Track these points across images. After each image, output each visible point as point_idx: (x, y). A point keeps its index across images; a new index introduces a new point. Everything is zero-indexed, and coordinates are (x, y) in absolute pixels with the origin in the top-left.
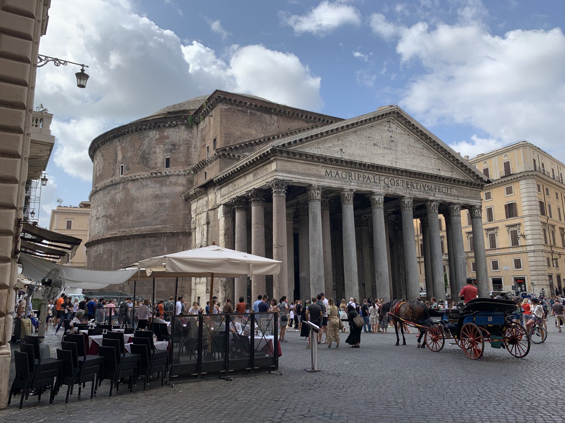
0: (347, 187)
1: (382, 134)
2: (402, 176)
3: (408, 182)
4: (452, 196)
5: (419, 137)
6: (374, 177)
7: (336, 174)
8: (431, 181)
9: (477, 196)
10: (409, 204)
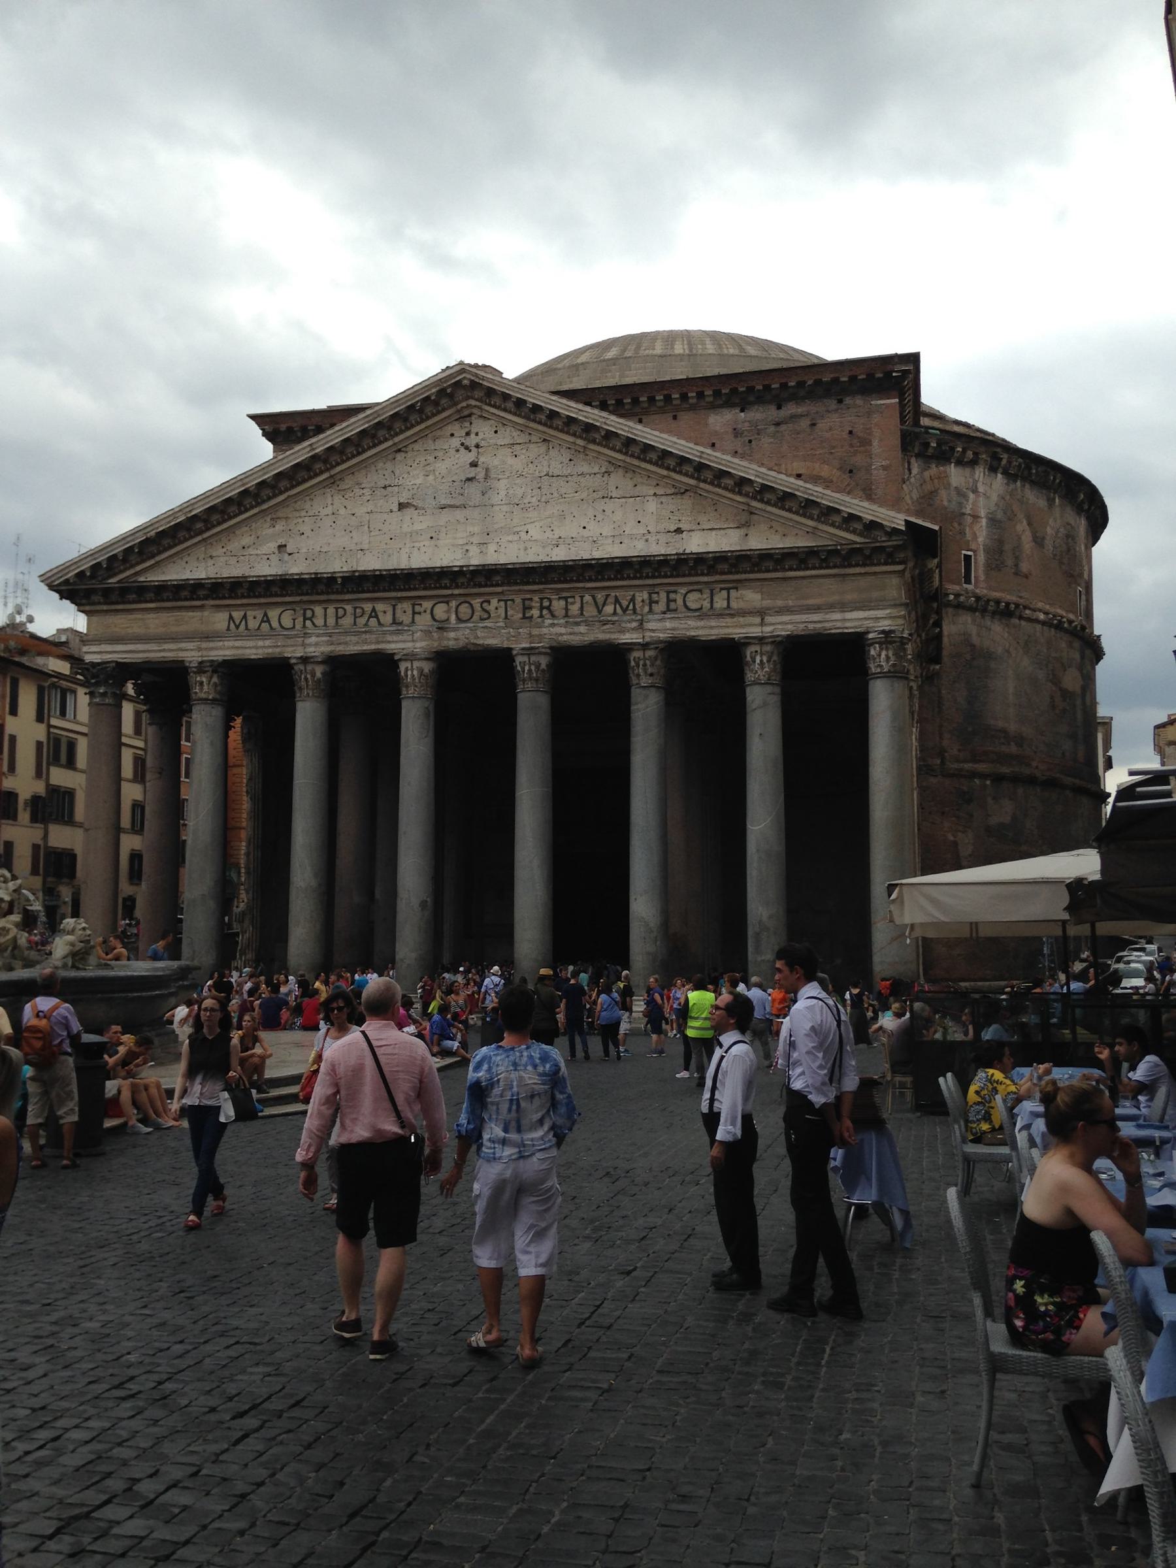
0: (293, 652)
1: (437, 465)
2: (492, 586)
3: (531, 599)
4: (732, 615)
5: (581, 437)
6: (394, 607)
7: (262, 621)
8: (623, 579)
9: (875, 594)
10: (524, 671)
